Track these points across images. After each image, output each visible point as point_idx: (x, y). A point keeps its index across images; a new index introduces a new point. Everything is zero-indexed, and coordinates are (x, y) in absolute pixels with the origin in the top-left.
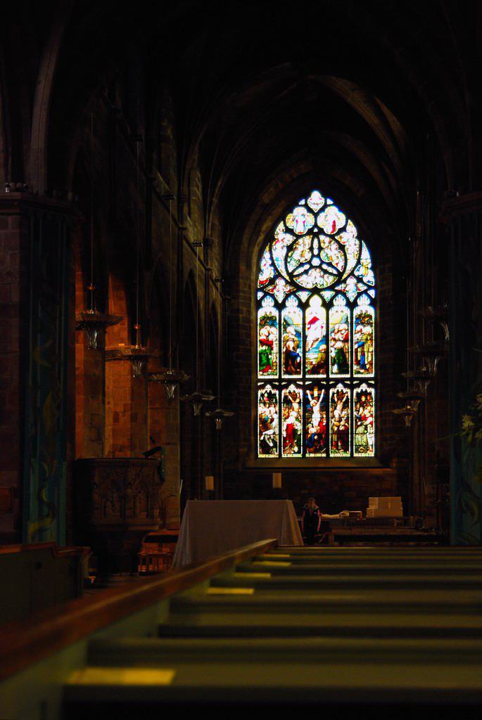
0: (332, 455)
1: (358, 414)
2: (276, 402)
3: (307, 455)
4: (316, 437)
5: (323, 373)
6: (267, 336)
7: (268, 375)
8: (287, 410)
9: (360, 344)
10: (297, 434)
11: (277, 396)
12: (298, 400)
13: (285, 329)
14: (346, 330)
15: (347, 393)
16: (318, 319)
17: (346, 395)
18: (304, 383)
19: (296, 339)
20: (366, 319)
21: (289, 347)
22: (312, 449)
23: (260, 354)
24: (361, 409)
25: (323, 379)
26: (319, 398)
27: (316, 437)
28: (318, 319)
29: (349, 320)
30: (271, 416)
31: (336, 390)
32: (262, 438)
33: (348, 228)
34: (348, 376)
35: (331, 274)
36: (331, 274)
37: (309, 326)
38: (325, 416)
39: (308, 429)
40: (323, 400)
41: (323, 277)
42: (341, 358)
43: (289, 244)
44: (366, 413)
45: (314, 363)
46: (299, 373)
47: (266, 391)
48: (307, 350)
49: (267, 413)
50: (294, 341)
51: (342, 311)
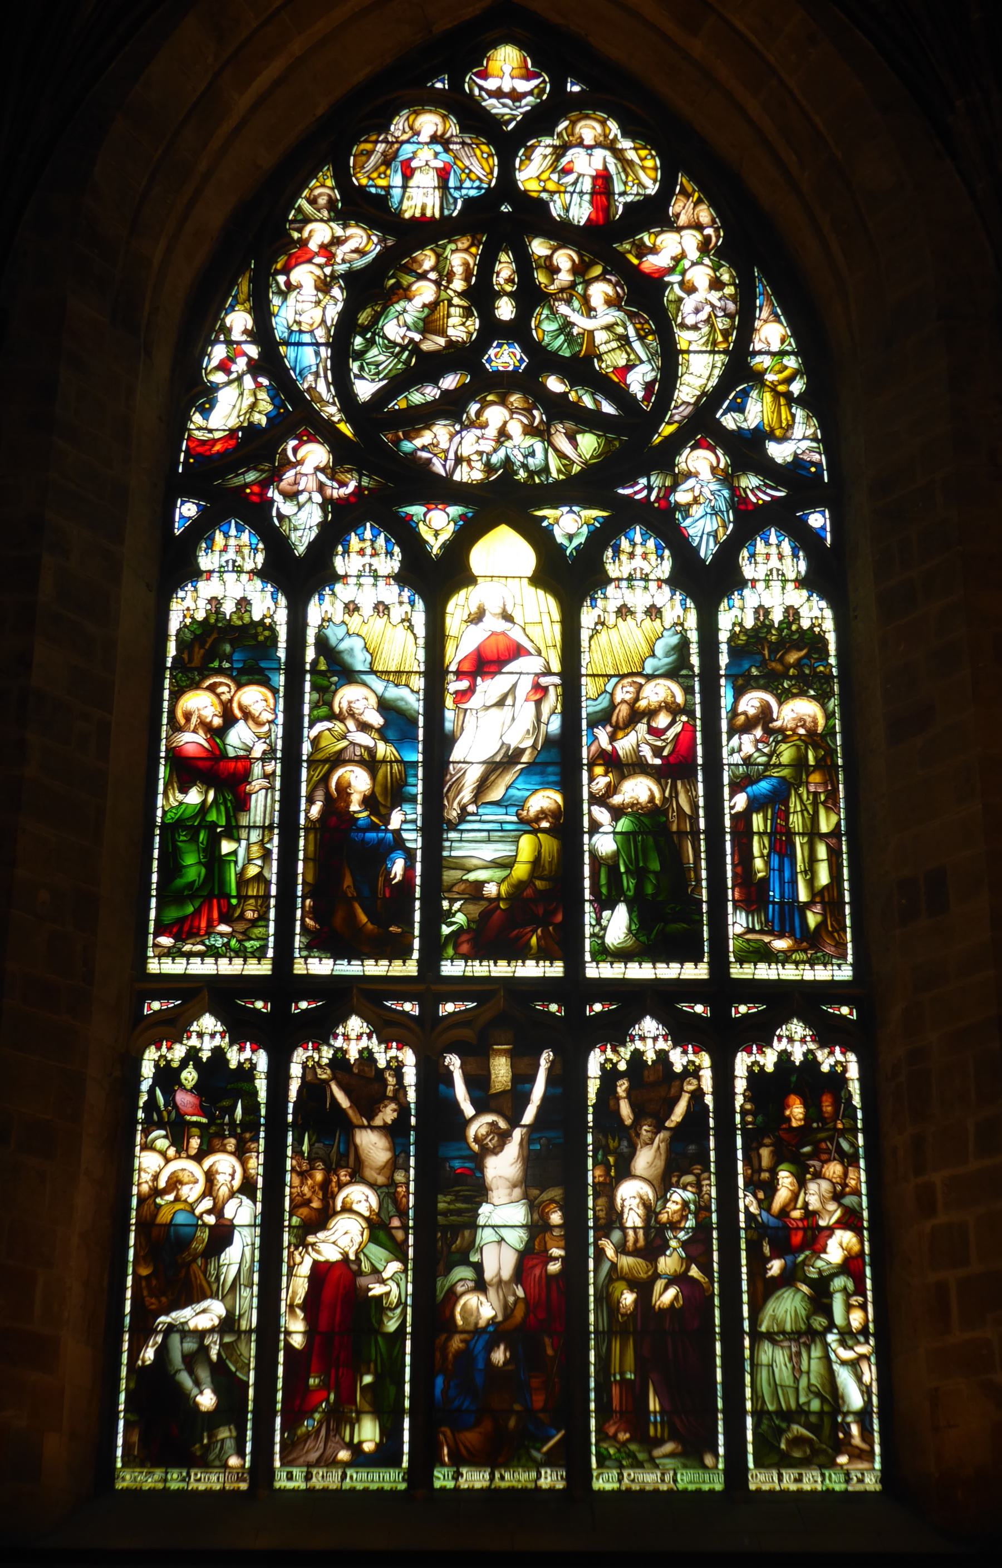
0: (604, 1482)
1: (765, 1204)
2: (251, 1124)
3: (442, 1479)
4: (499, 1356)
5: (543, 955)
6: (217, 733)
7: (214, 953)
8: (319, 1176)
9: (764, 786)
10: (376, 1329)
11: (261, 1085)
12: (388, 1114)
13: (325, 693)
14: (674, 710)
15: (692, 1072)
16: (517, 651)
17: (690, 1086)
18: (429, 1007)
19: (383, 750)
20: (792, 657)
21: (344, 790)
22: (471, 1437)
23: (170, 829)
24: (785, 1179)
25: (543, 987)
26: (517, 1096)
27: (499, 1356)
28: (517, 651)
29: (695, 660)
30: (217, 1210)
31: (626, 1052)
32: (149, 1354)
33: (681, 209)
34: (697, 971)
35: (592, 421)
36: (592, 421)
37: (464, 684)
38: (556, 1218)
39: (452, 1297)
40: (541, 1109)
41: (541, 433)
42: (655, 865)
43: (360, 263)
44: (815, 1194)
45: (491, 890)
46: (405, 955)
47: (193, 1054)
48: (453, 814)
49: (191, 1192)
50: (370, 763)
51: (654, 612)
